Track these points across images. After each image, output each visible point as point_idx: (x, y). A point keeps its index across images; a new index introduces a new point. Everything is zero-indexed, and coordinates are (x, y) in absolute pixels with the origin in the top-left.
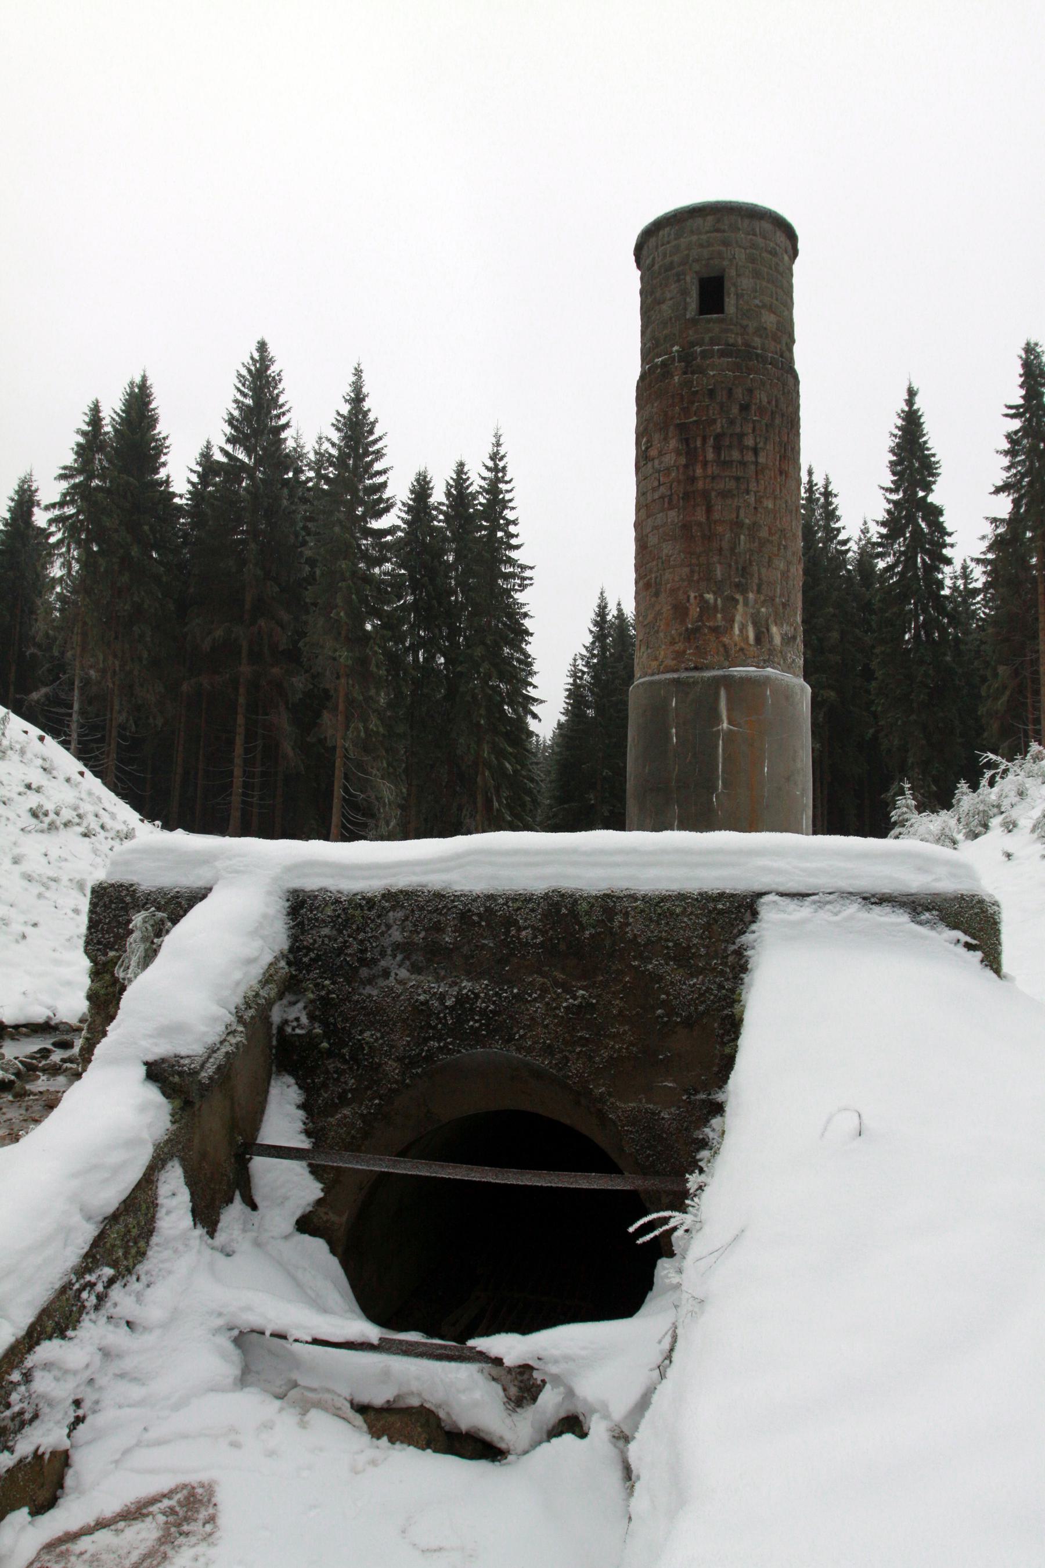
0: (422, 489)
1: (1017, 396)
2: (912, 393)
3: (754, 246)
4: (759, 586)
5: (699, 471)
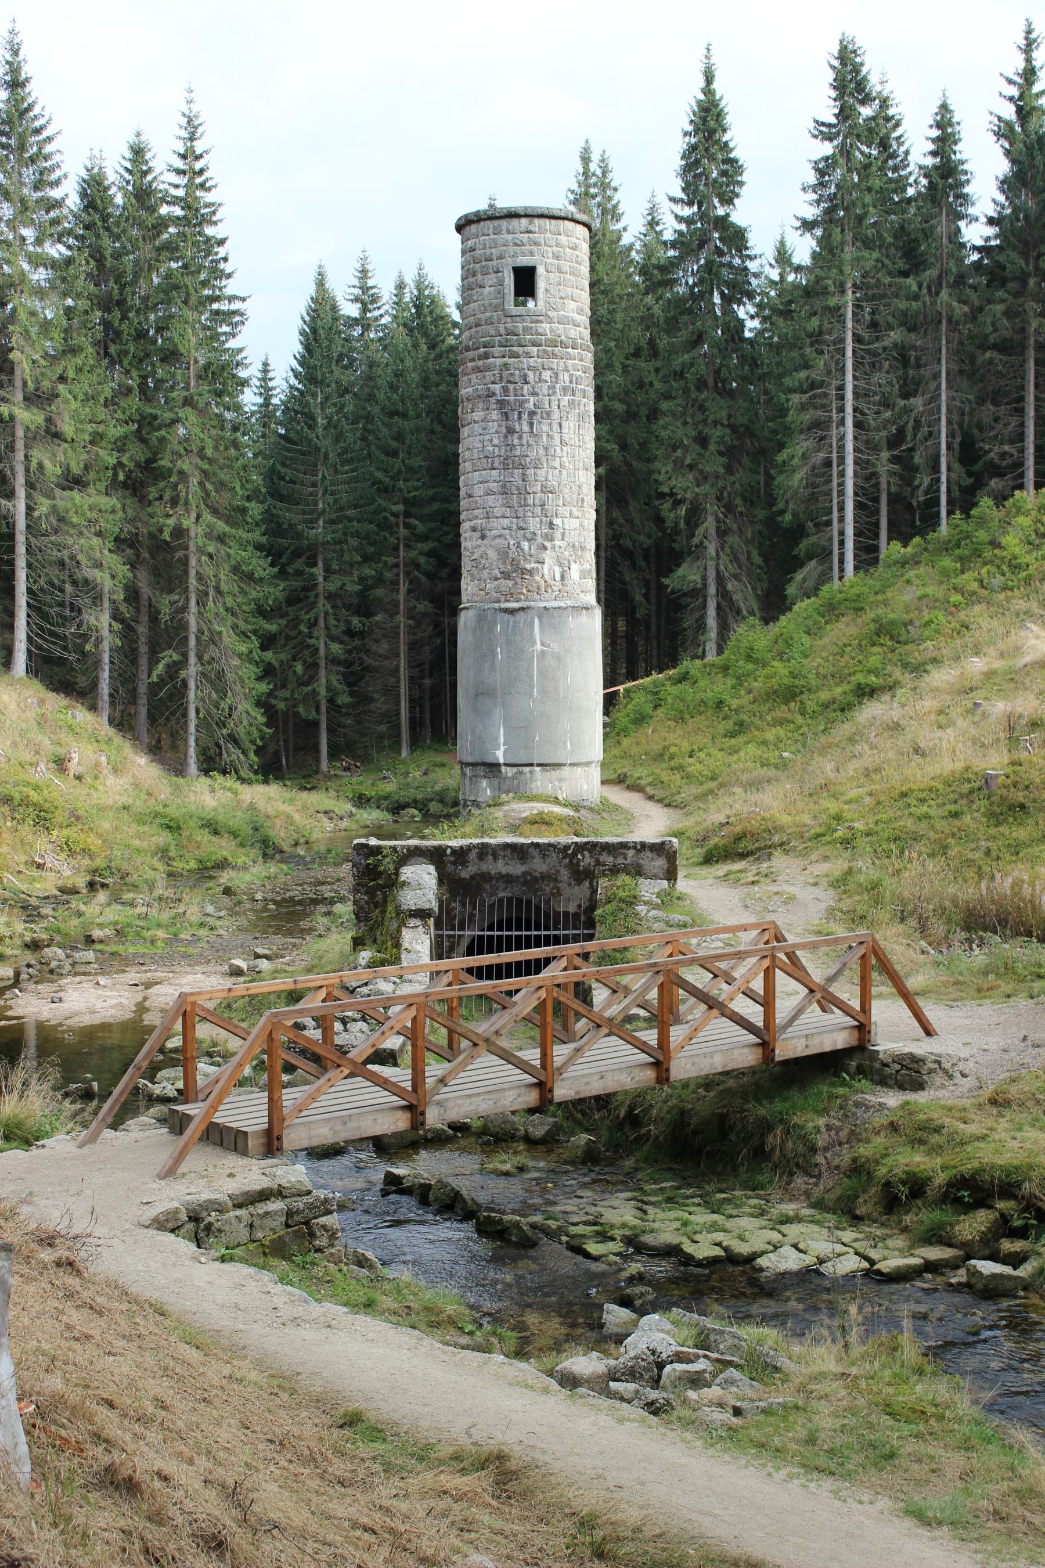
0: (94, 190)
2: (709, 77)
3: (558, 245)
4: (563, 534)
5: (516, 442)
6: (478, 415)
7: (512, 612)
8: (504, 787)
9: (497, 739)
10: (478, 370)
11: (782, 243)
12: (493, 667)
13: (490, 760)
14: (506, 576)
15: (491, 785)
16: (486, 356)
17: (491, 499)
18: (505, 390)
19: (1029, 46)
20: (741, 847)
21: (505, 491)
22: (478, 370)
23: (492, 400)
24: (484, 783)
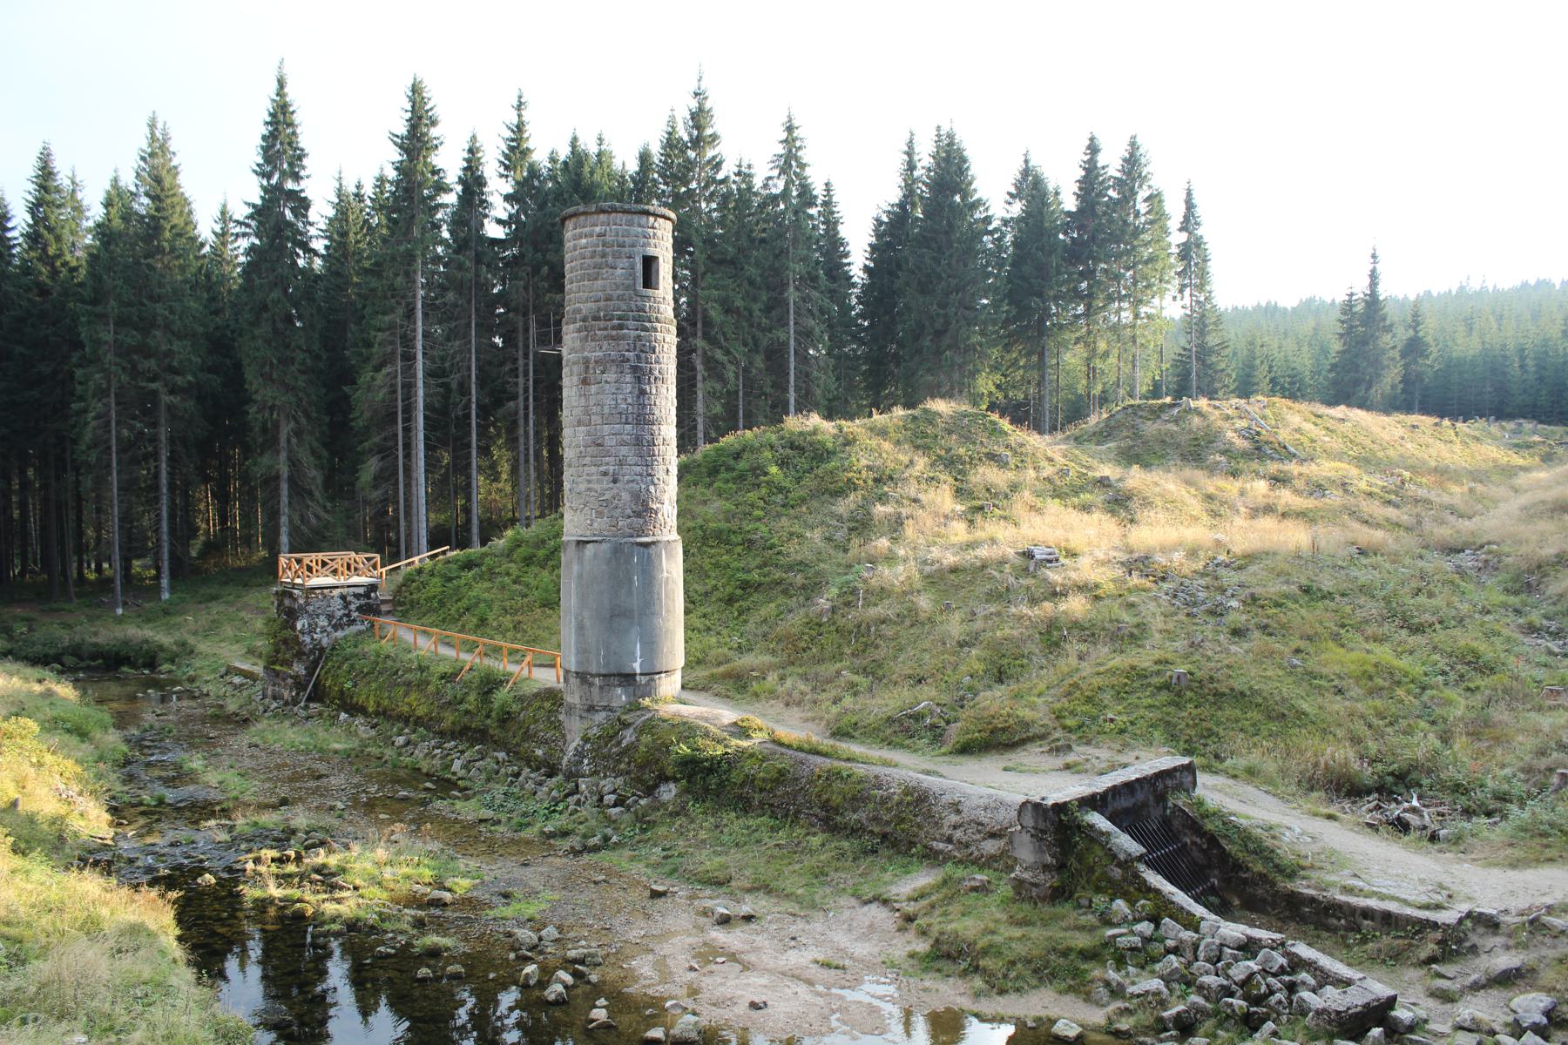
1: (402, 129)
2: (281, 84)
6: (611, 376)
7: (646, 545)
8: (639, 693)
9: (634, 653)
10: (613, 338)
11: (224, 206)
12: (630, 592)
13: (628, 671)
14: (638, 515)
15: (626, 693)
16: (621, 327)
17: (624, 450)
18: (638, 357)
19: (520, 106)
20: (1004, 738)
21: (638, 442)
22: (613, 338)
23: (627, 365)
24: (619, 691)
